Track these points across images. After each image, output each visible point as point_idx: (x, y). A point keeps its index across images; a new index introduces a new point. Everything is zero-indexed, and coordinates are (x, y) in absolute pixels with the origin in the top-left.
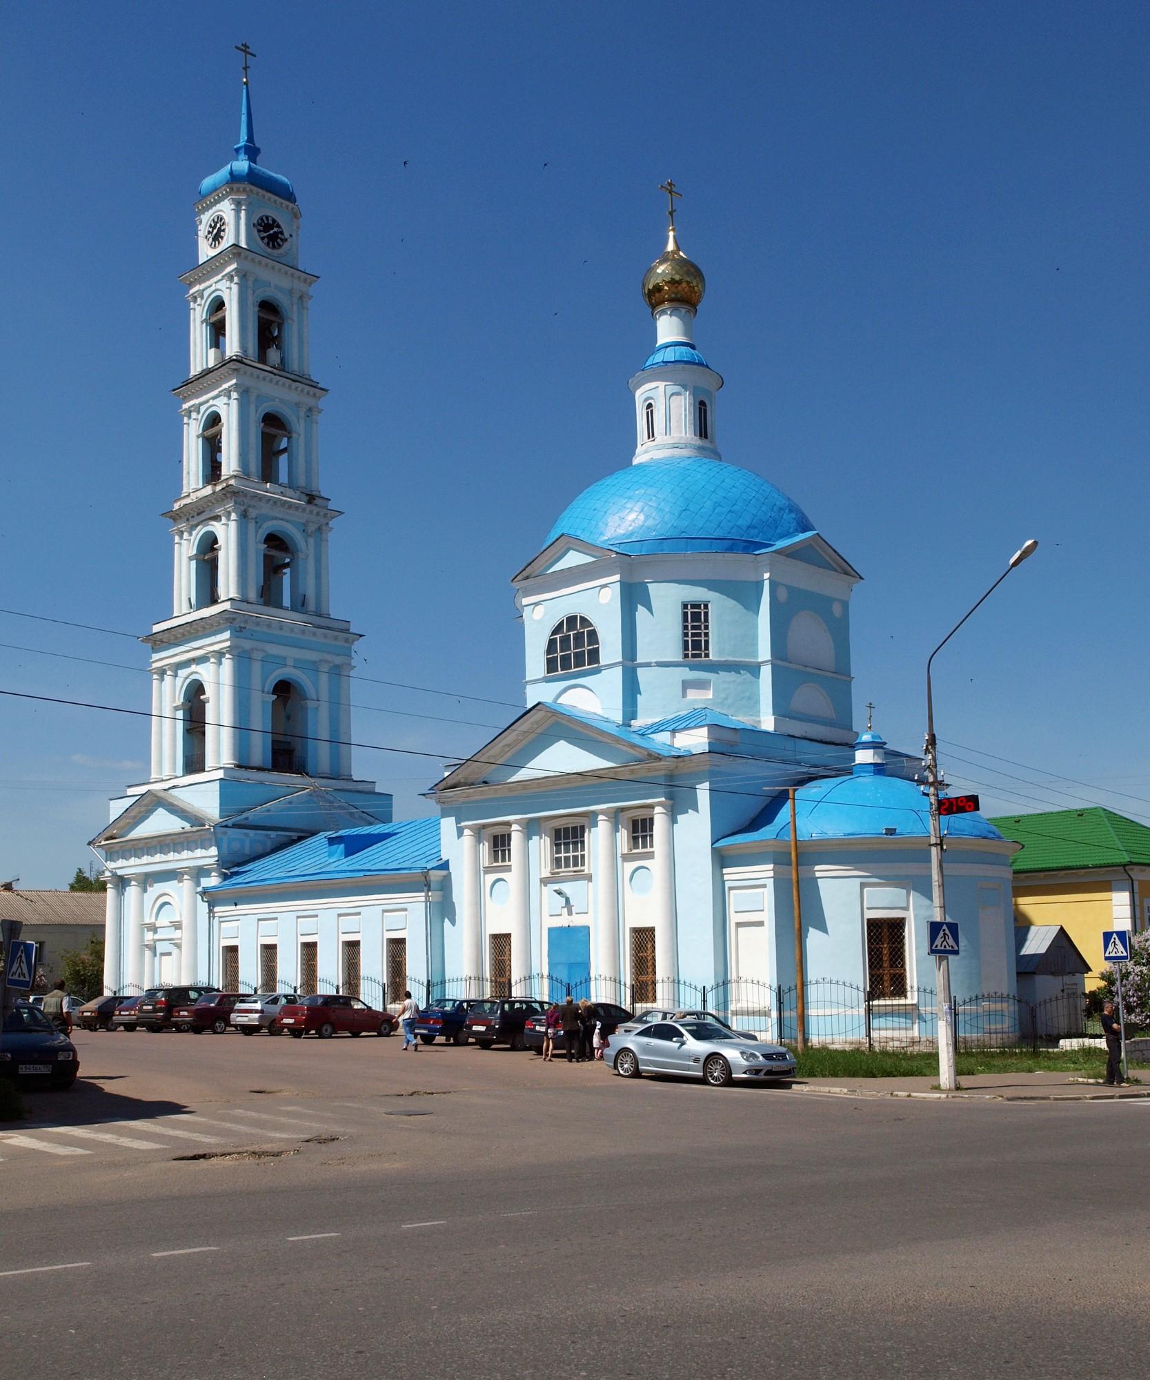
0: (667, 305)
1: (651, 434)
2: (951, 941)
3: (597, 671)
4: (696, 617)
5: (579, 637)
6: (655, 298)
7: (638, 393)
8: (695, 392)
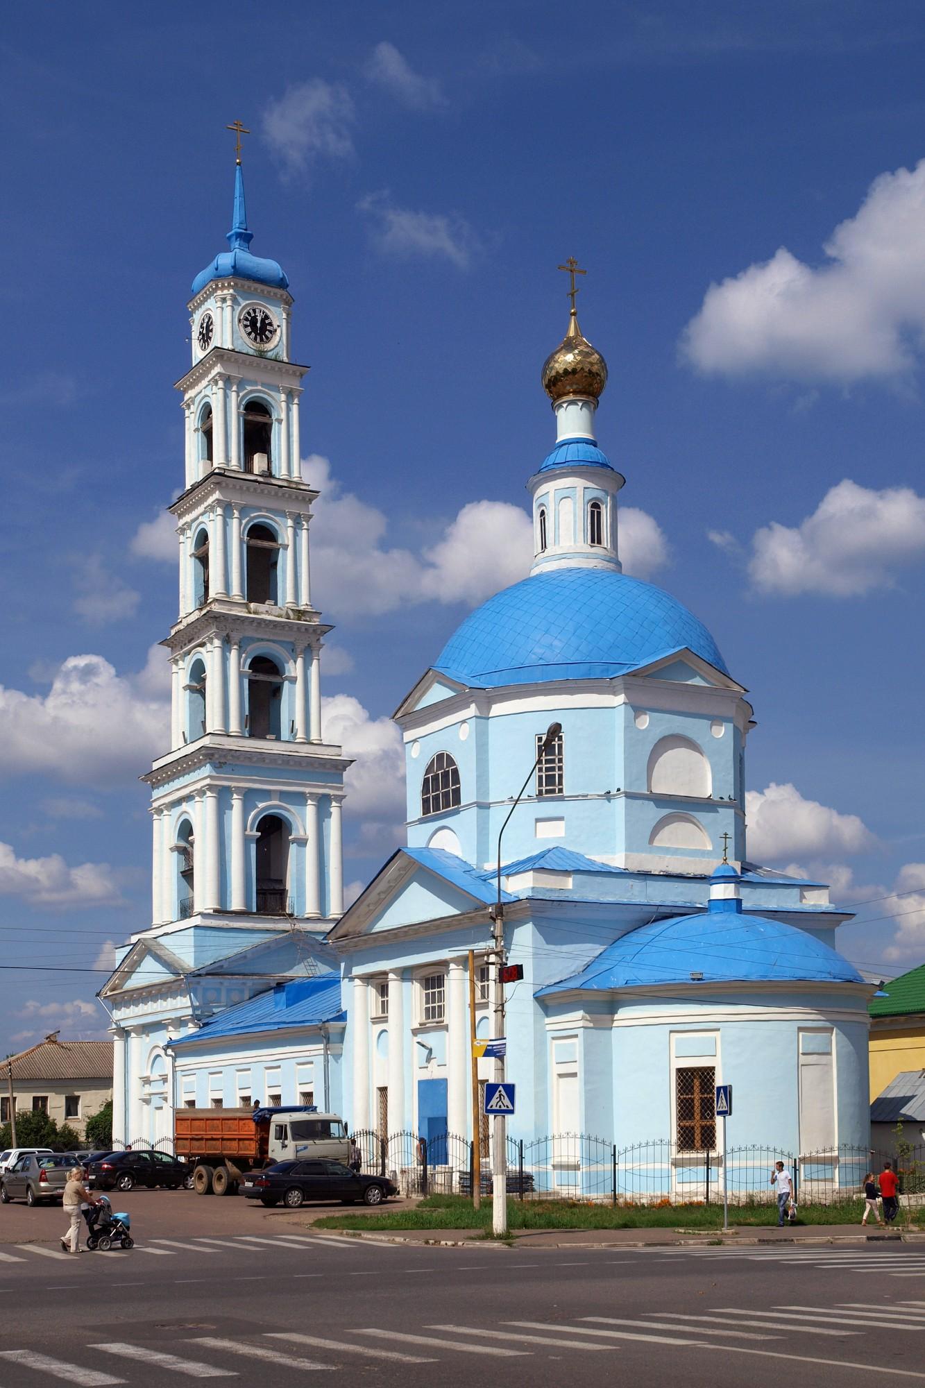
2: (507, 1101)
3: (457, 812)
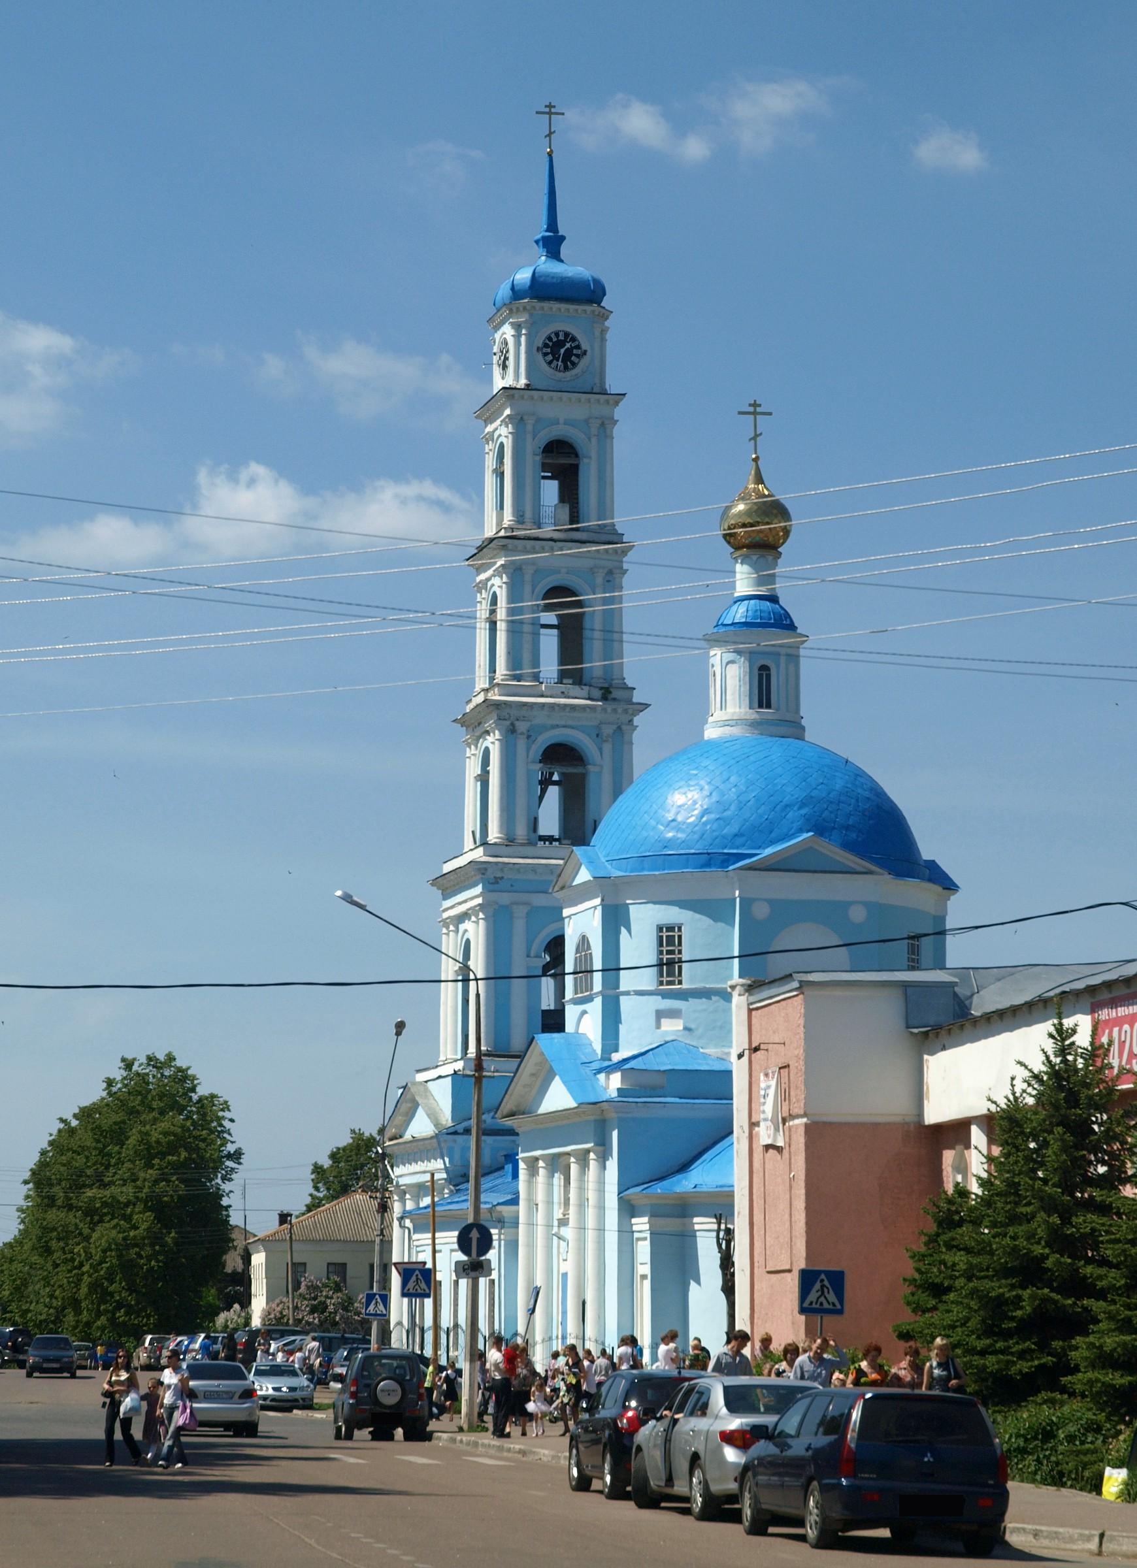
4: (670, 941)
8: (751, 655)
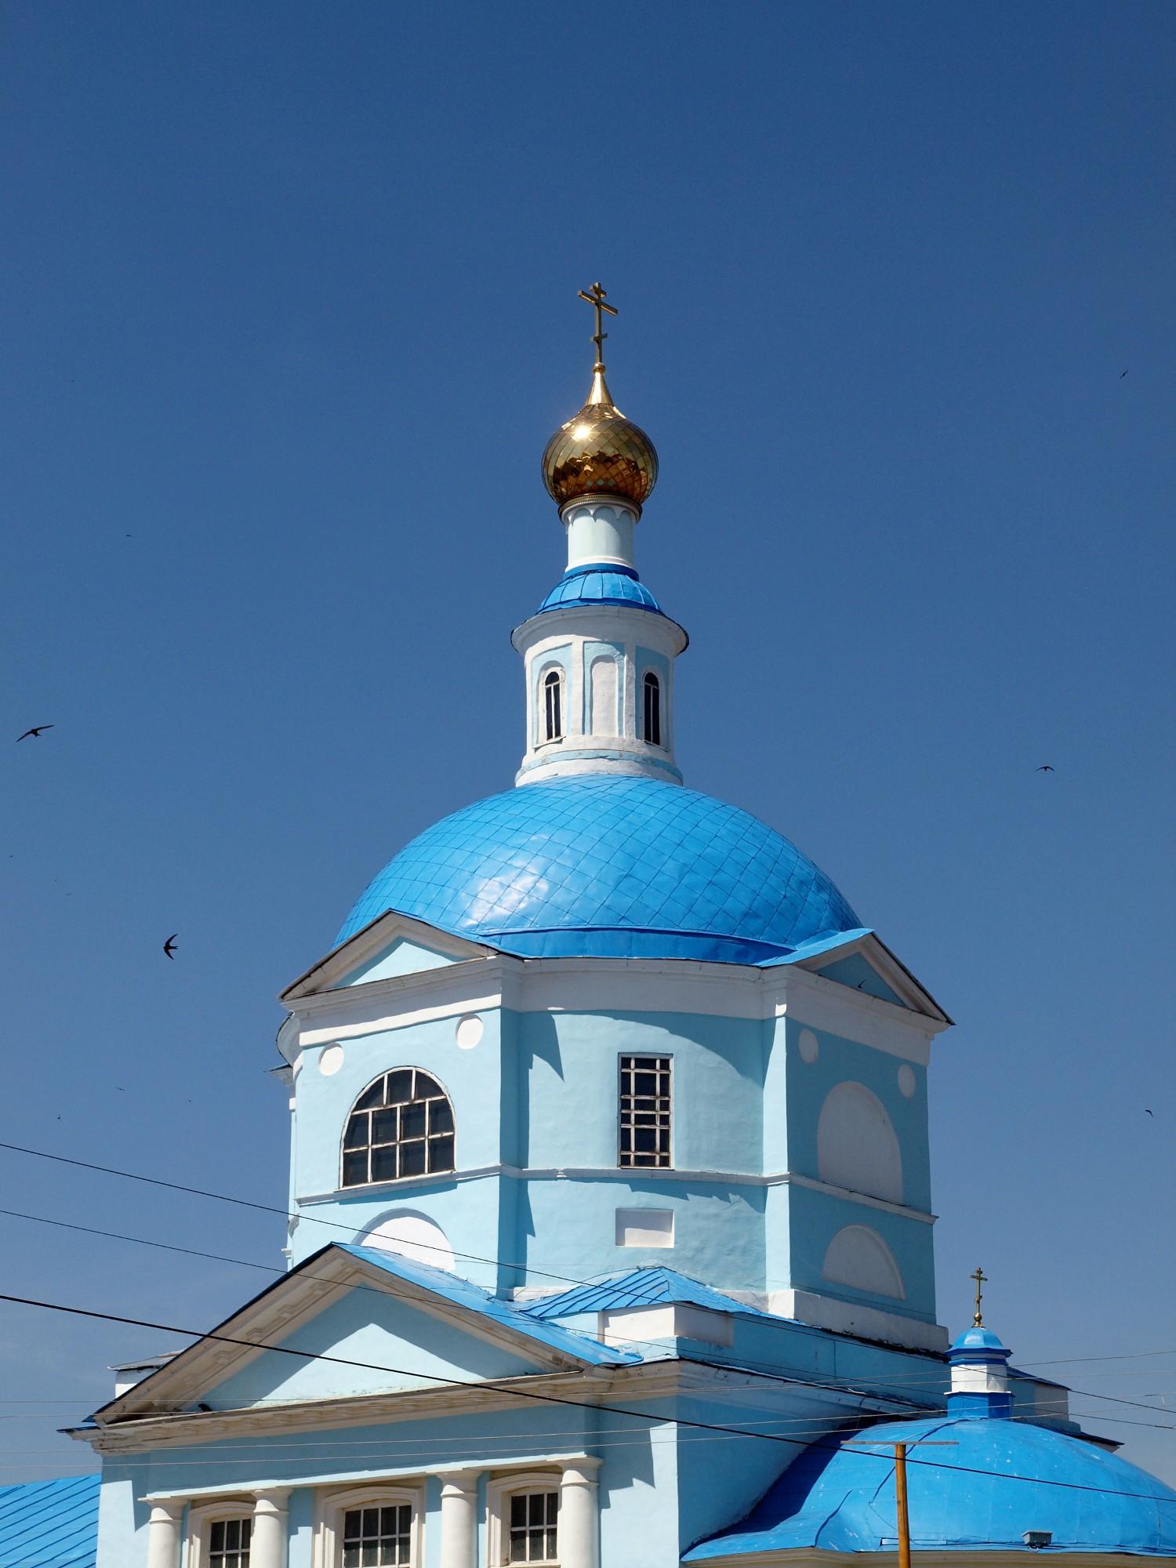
0: (587, 499)
1: (554, 730)
3: (449, 1184)
4: (645, 1084)
5: (413, 1116)
6: (568, 485)
7: (531, 654)
8: (640, 657)
